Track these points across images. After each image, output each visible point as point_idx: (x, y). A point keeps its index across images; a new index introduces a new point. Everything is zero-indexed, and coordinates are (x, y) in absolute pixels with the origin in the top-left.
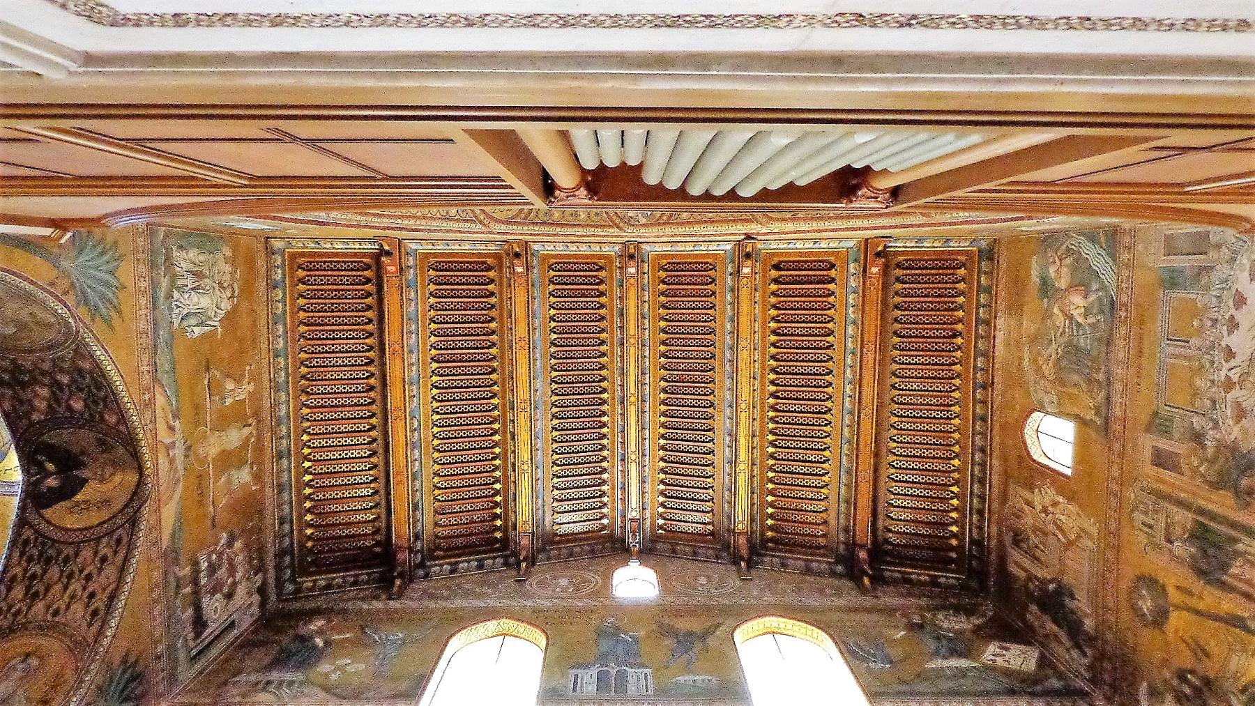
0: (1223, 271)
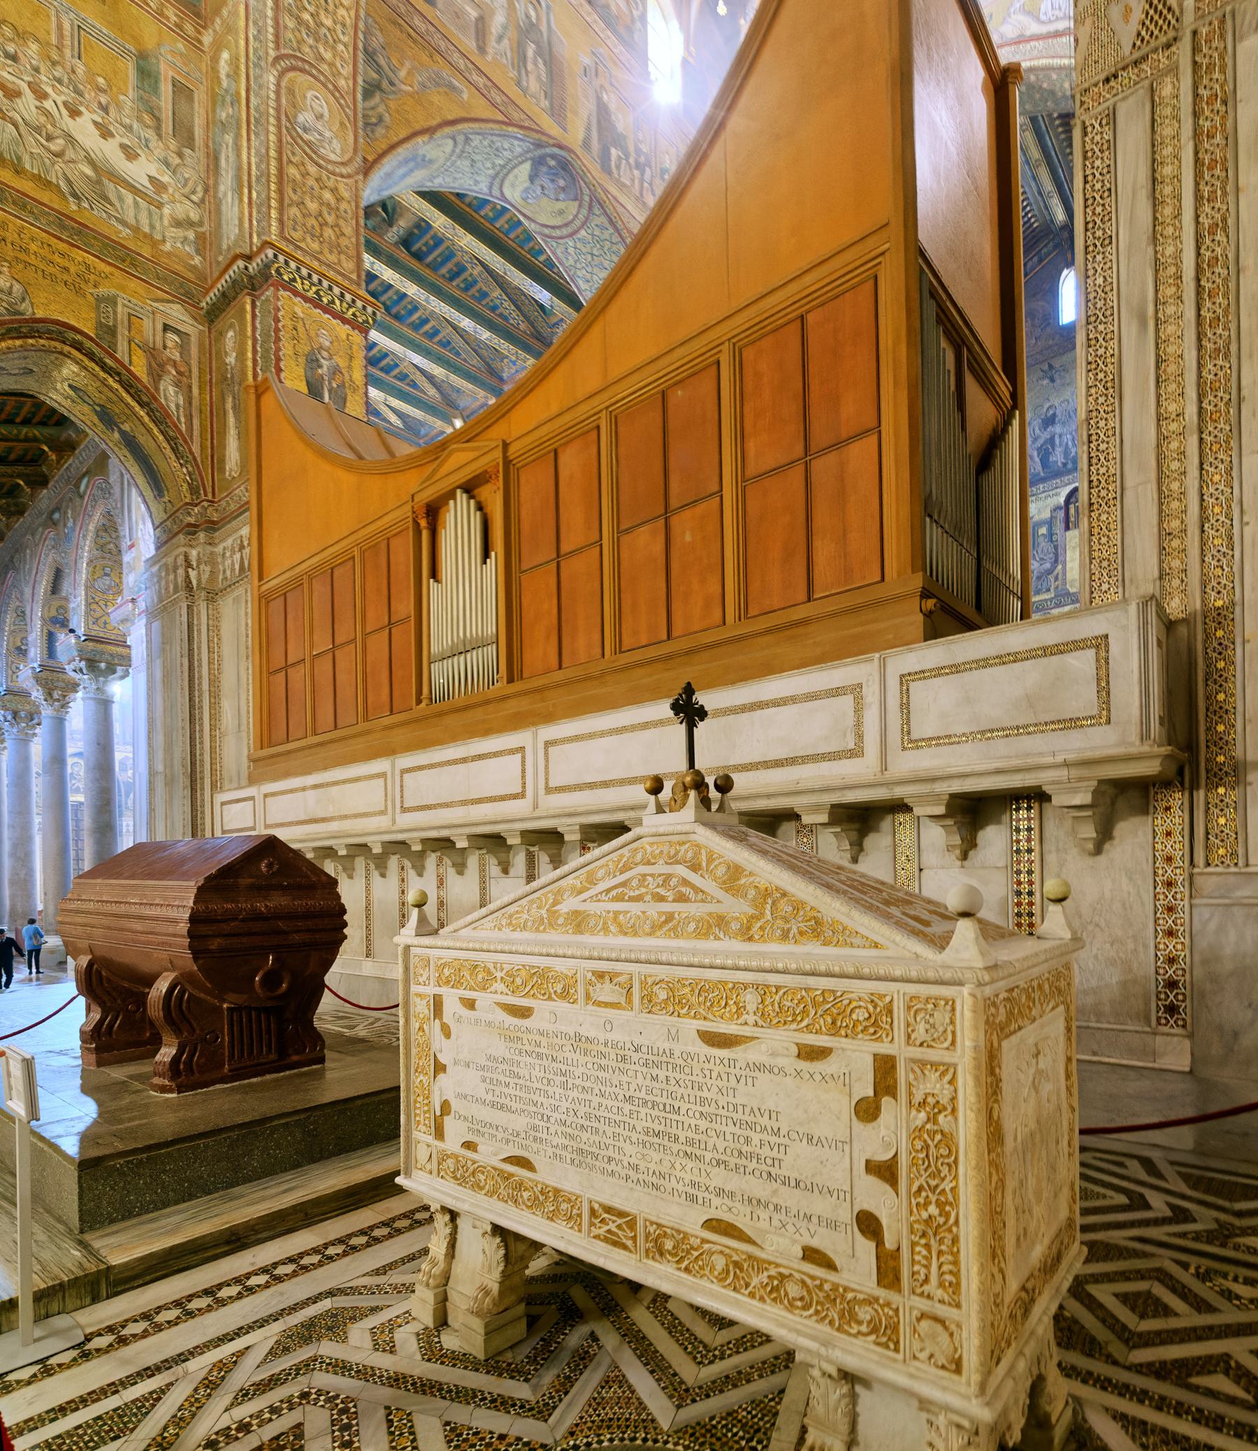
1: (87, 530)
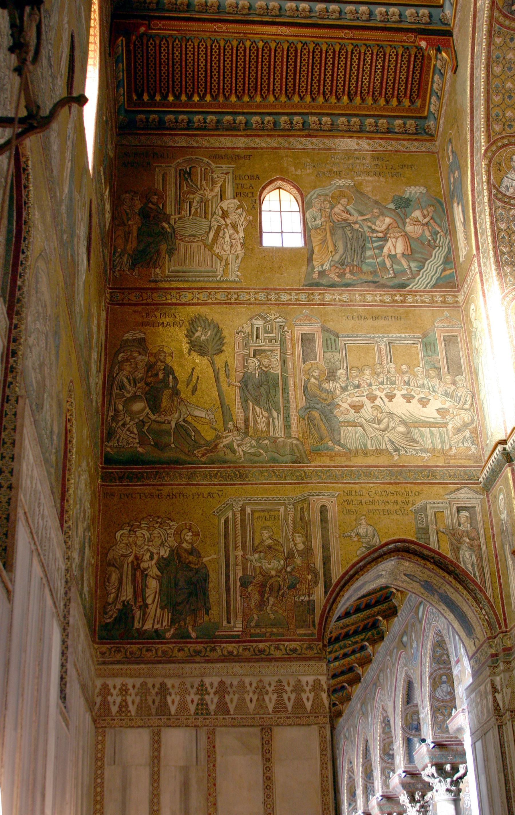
0: (440, 388)
1: (426, 648)
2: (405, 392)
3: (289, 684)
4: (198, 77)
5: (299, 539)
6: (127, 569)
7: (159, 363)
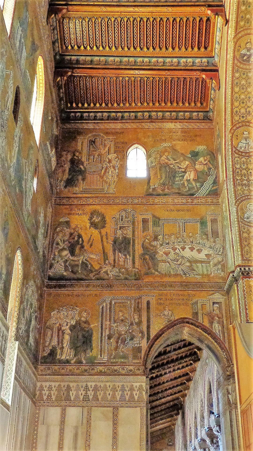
2: (191, 246)
3: (127, 387)
4: (99, 95)
5: (136, 317)
6: (55, 330)
7: (76, 233)
